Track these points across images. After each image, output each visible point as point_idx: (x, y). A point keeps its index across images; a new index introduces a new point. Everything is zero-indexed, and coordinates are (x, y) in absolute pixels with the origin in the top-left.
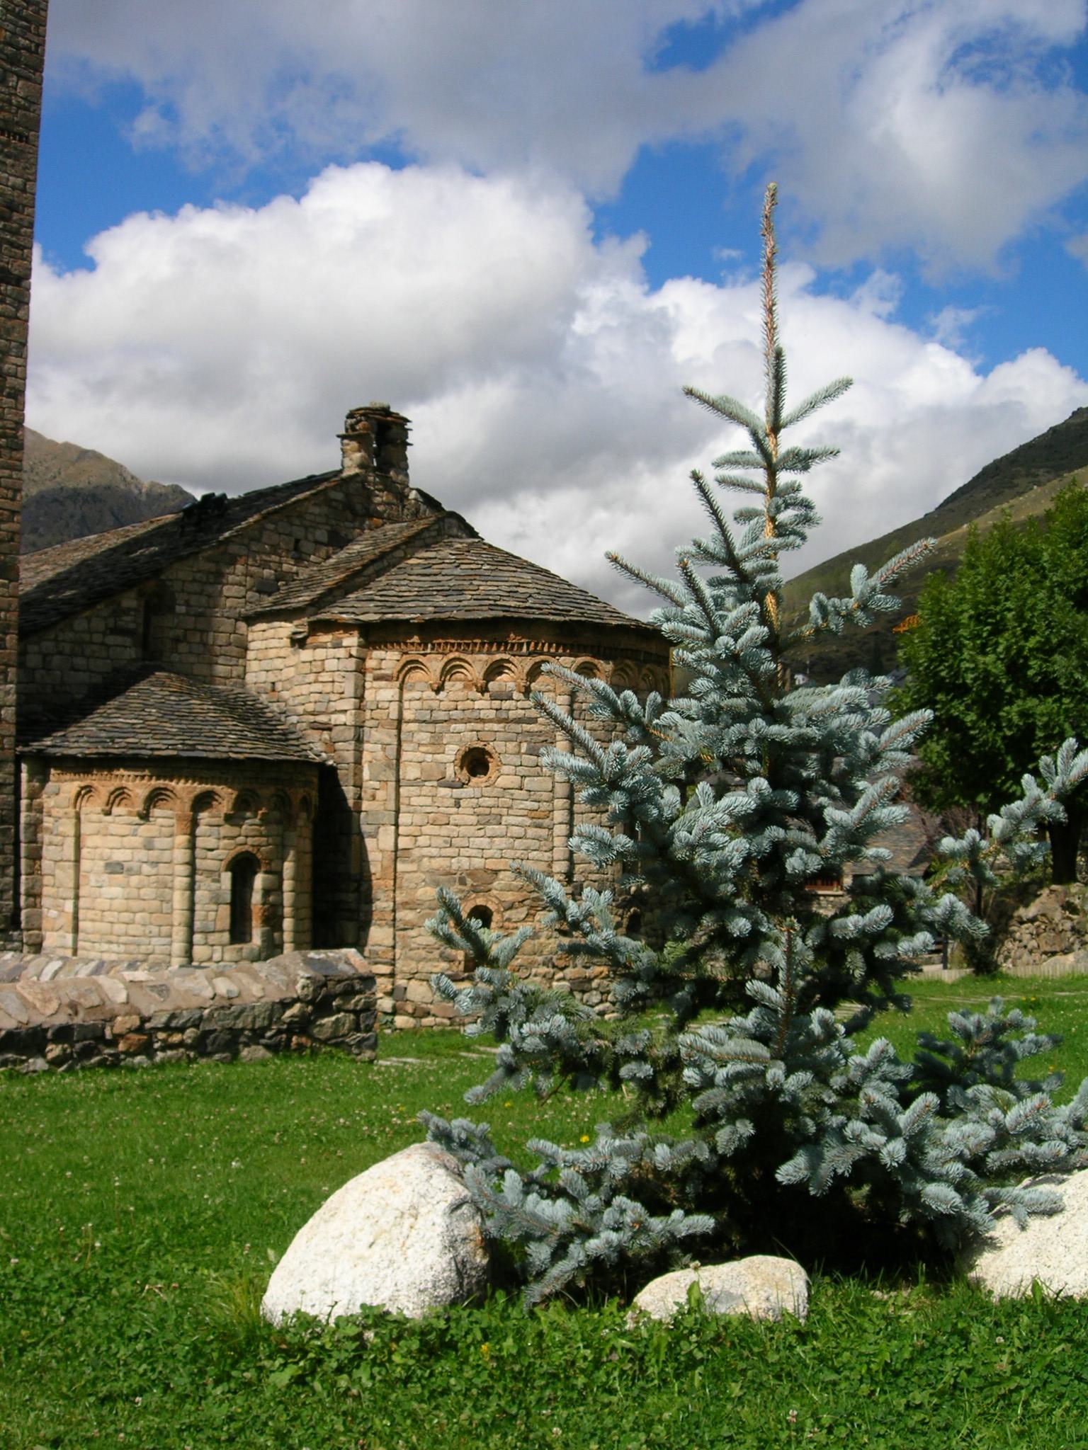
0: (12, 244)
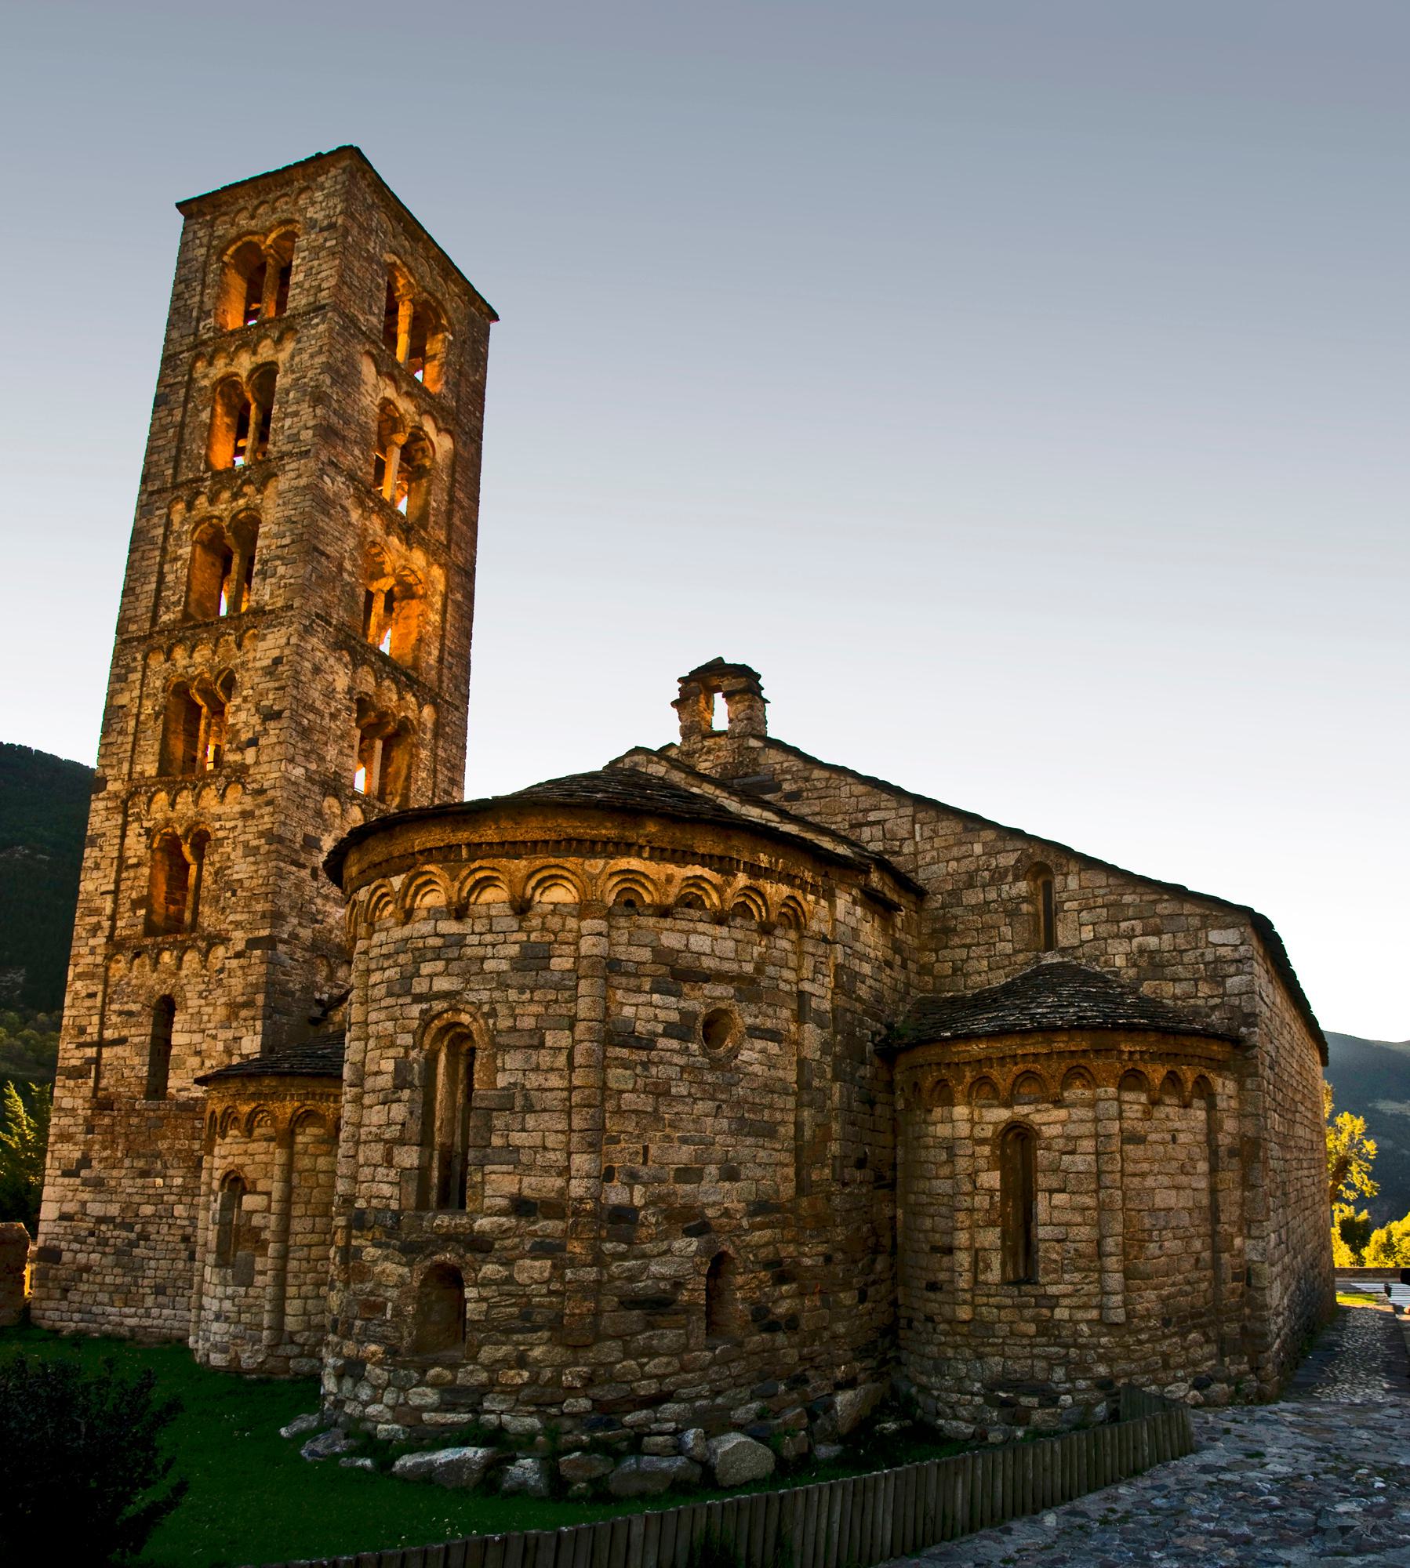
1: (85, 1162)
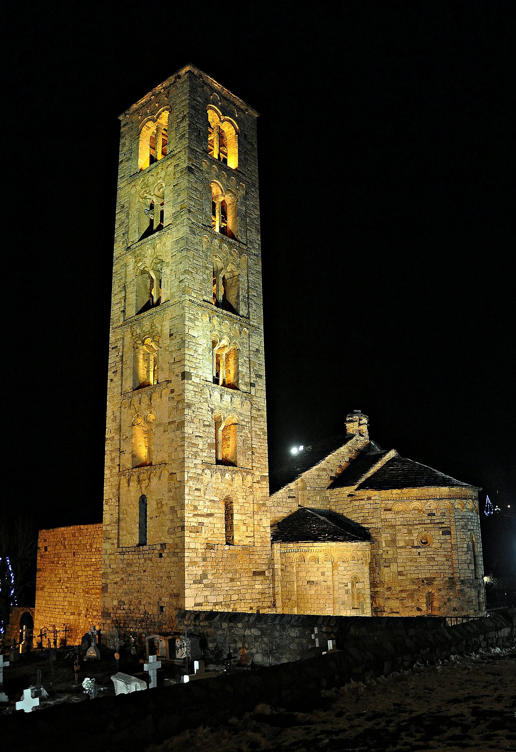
1: (204, 576)
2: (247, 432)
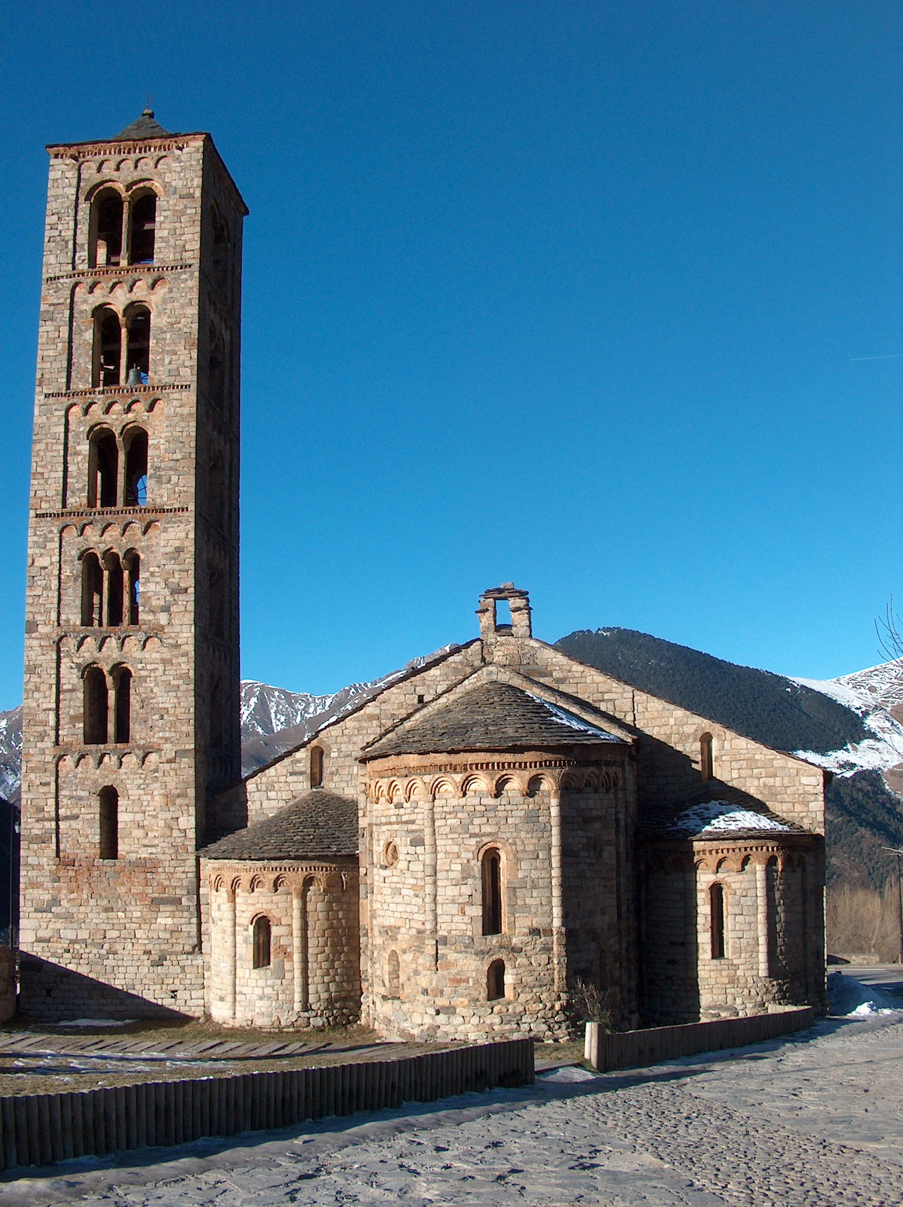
0: (180, 571)
1: (56, 902)
2: (152, 685)
